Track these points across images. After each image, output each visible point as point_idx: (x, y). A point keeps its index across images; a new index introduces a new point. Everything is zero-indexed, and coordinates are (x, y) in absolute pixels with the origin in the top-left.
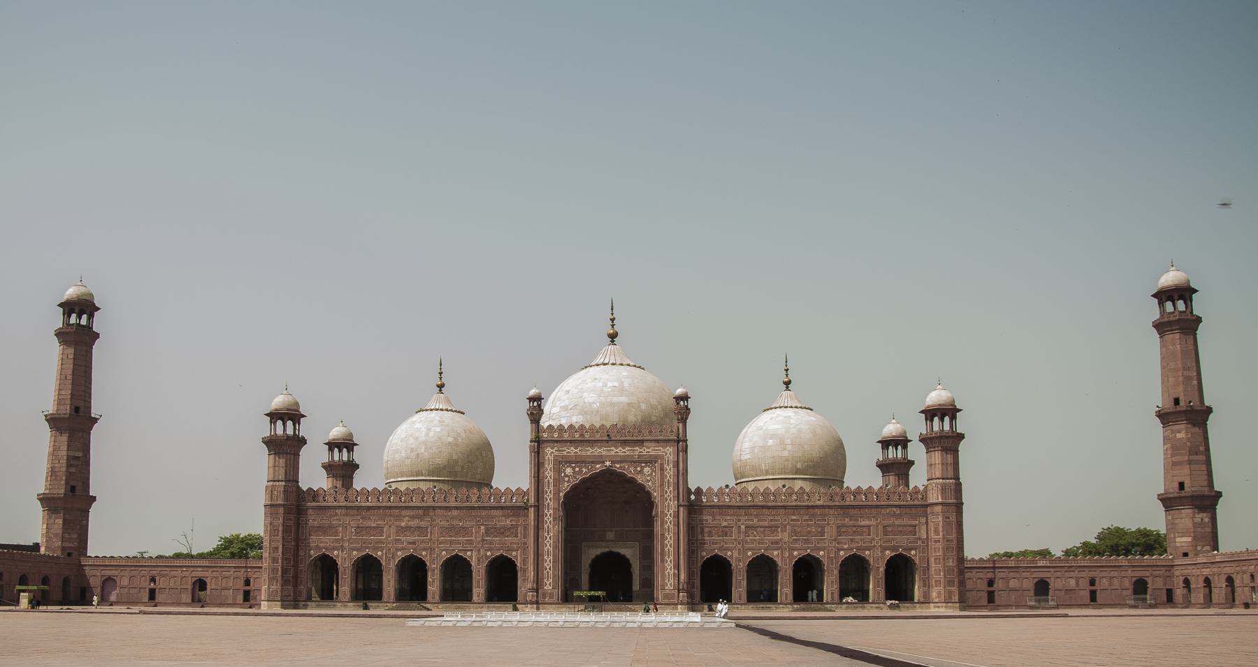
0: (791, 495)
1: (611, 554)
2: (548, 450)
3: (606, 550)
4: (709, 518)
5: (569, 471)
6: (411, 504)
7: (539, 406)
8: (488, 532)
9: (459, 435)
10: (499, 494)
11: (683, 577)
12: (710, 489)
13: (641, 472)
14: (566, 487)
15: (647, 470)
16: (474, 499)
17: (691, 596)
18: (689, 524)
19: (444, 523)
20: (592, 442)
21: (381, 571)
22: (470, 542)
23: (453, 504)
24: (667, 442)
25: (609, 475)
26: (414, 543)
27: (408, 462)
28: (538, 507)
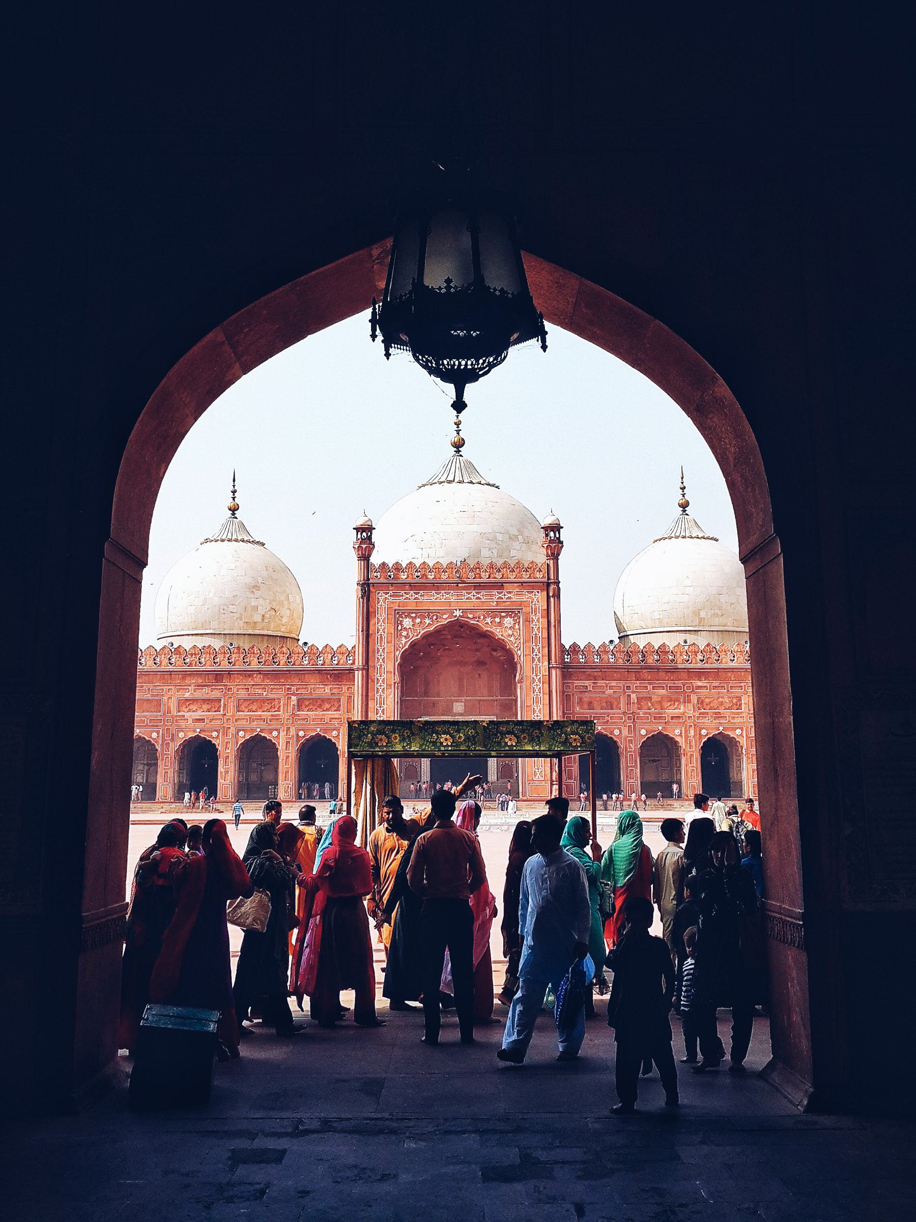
0: (696, 653)
5: (407, 622)
7: (370, 538)
8: (300, 704)
10: (312, 652)
12: (589, 645)
14: (405, 643)
15: (508, 621)
16: (283, 659)
18: (563, 692)
19: (243, 694)
20: (436, 586)
22: (276, 718)
23: (254, 666)
24: (530, 586)
27: (191, 610)
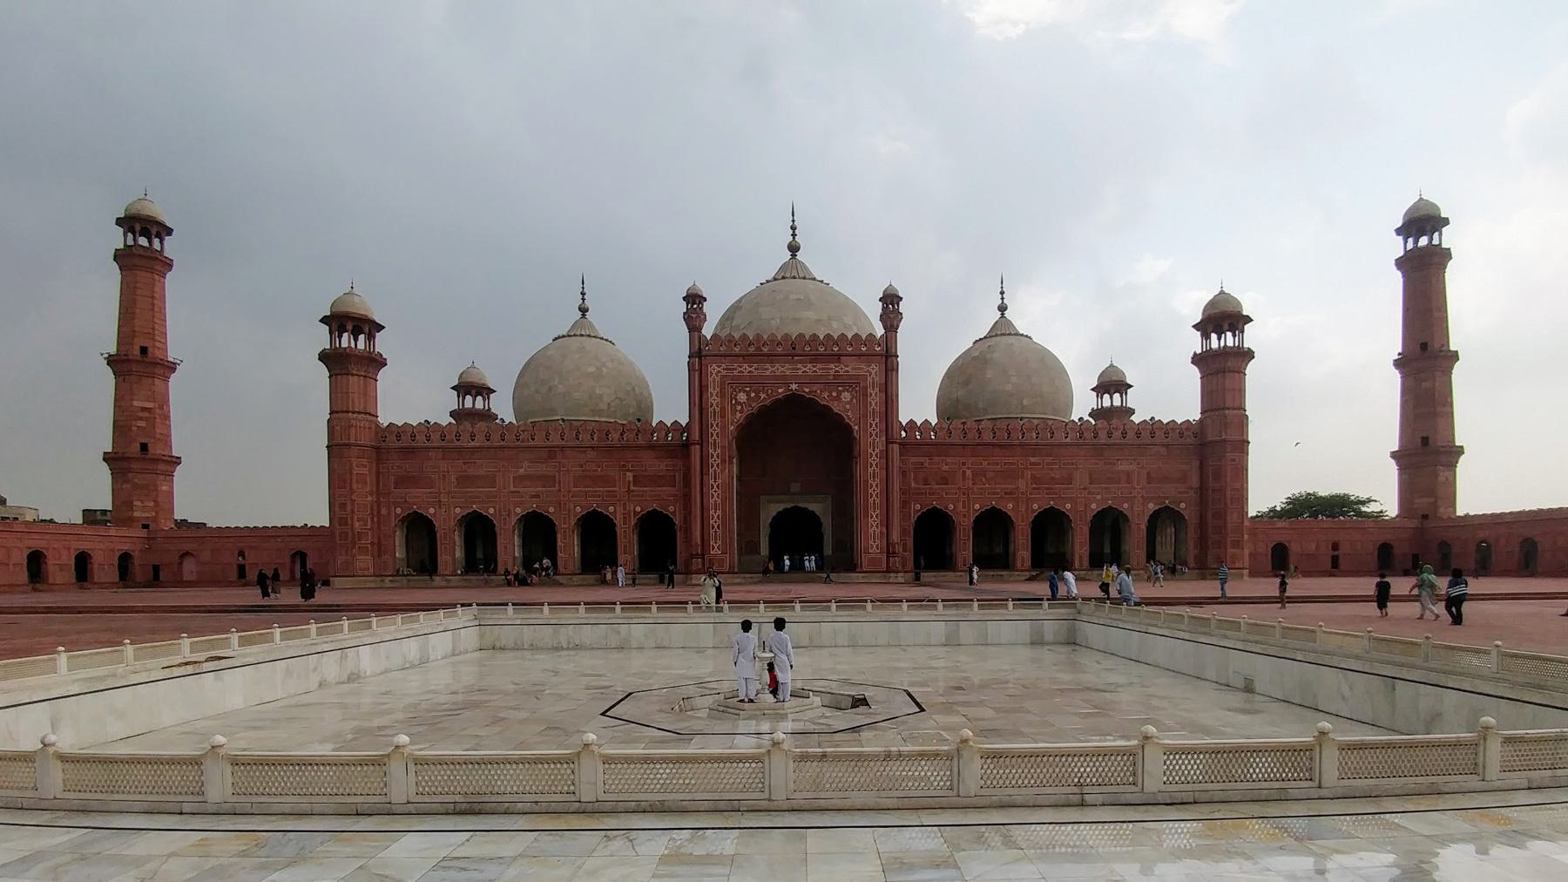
0: (1030, 430)
1: (796, 508)
2: (713, 369)
3: (789, 506)
4: (926, 461)
5: (742, 397)
6: (532, 443)
8: (636, 481)
9: (604, 365)
11: (895, 536)
13: (838, 398)
15: (846, 396)
16: (615, 436)
17: (904, 564)
21: (494, 535)
24: (869, 356)
25: (794, 400)
26: (537, 496)
28: (702, 442)
